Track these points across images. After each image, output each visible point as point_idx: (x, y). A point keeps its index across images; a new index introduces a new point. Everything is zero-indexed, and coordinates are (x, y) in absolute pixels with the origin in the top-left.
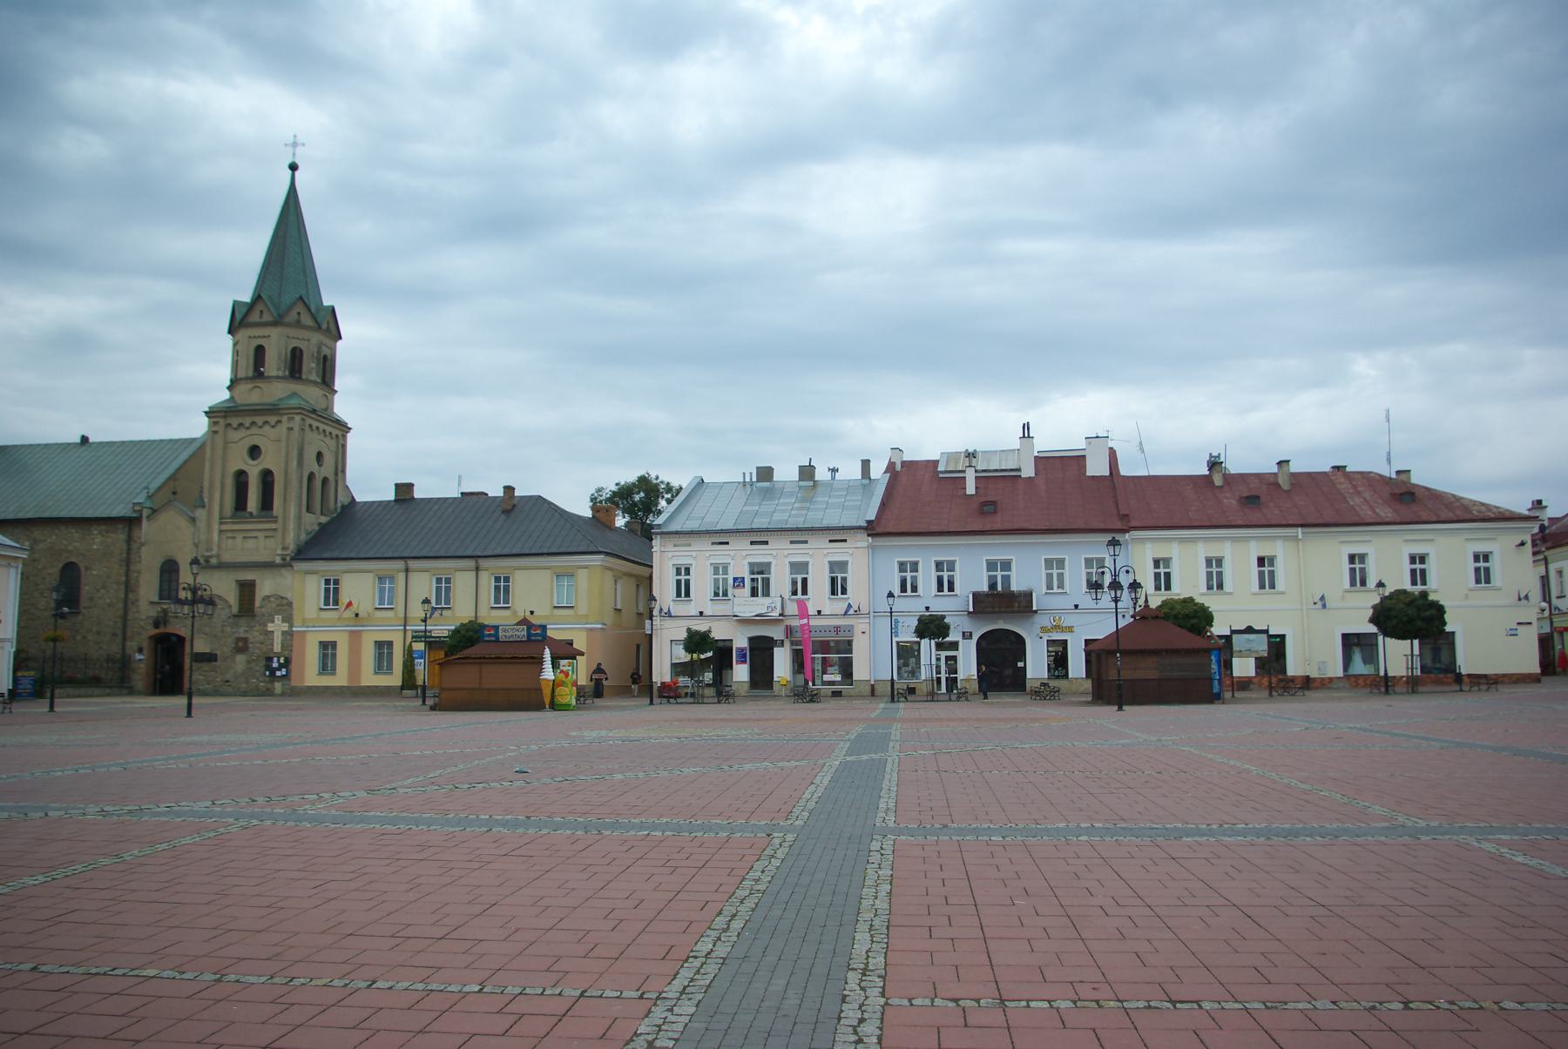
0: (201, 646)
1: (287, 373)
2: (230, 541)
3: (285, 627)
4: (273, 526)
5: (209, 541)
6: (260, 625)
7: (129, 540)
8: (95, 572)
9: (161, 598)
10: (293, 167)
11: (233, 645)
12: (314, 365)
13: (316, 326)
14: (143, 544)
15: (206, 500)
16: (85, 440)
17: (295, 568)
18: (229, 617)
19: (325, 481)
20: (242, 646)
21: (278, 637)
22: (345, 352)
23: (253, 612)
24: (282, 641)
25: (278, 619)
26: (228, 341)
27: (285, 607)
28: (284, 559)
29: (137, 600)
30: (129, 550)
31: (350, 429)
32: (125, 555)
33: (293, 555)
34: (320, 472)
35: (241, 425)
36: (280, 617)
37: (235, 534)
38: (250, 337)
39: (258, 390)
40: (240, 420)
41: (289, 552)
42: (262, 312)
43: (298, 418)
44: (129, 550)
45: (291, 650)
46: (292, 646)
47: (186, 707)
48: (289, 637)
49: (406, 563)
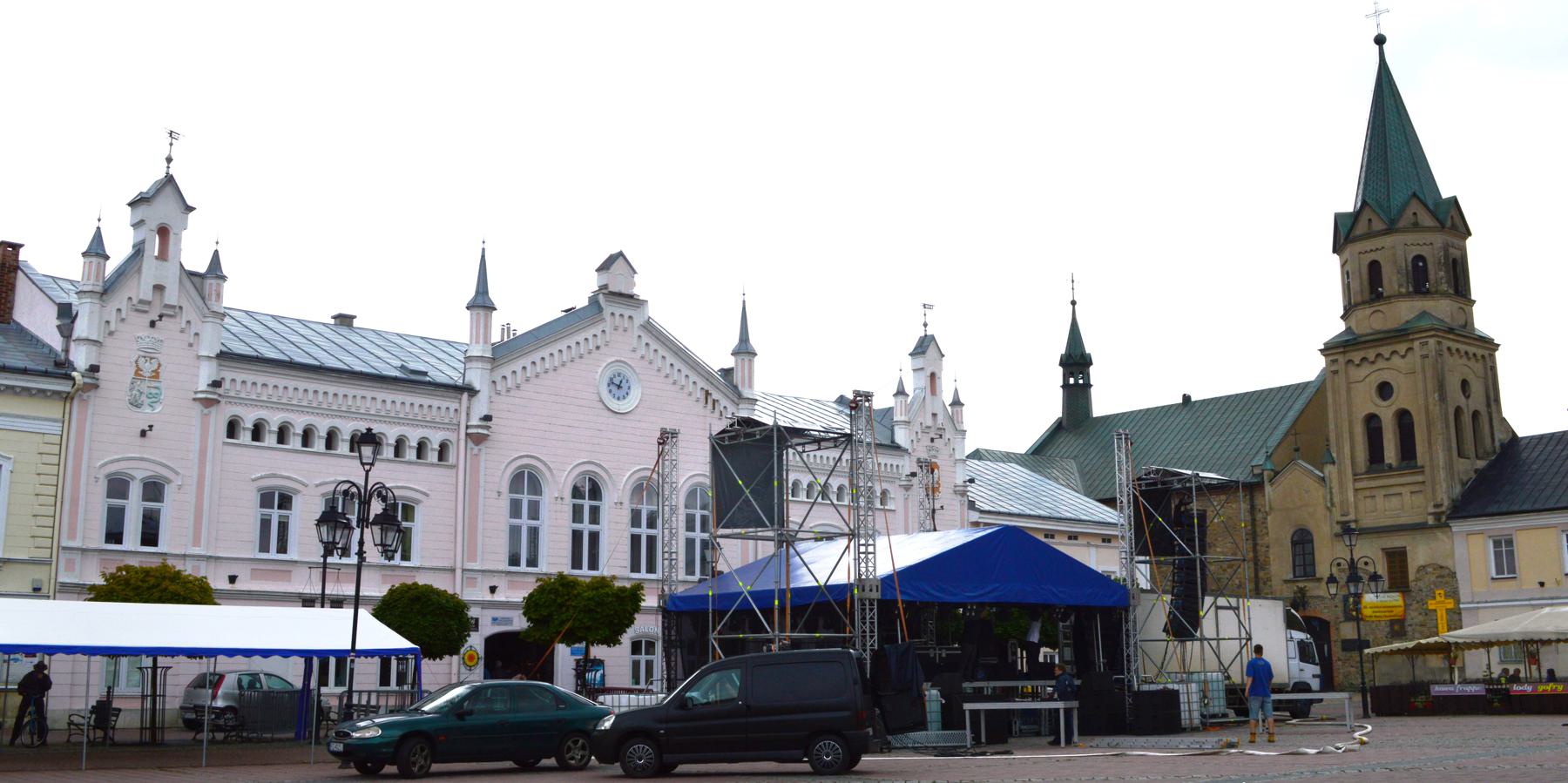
1: (1411, 289)
2: (1369, 500)
3: (1450, 604)
4: (1420, 478)
5: (1344, 502)
6: (1418, 602)
7: (1253, 509)
8: (1218, 550)
9: (1295, 576)
10: (1380, 40)
11: (1388, 629)
12: (1442, 274)
13: (1438, 225)
14: (1267, 514)
15: (1334, 455)
16: (1186, 398)
17: (1454, 529)
19: (1476, 415)
21: (1442, 616)
26: (1335, 260)
27: (1446, 578)
28: (1439, 520)
29: (1269, 579)
30: (1254, 520)
31: (1498, 345)
32: (1250, 527)
33: (1448, 512)
34: (1468, 405)
35: (1364, 359)
36: (1442, 592)
37: (1374, 492)
38: (1360, 253)
39: (1380, 314)
40: (1361, 354)
41: (1444, 509)
42: (1370, 220)
43: (1432, 341)
44: (1254, 520)
47: (1361, 704)
48: (1456, 617)
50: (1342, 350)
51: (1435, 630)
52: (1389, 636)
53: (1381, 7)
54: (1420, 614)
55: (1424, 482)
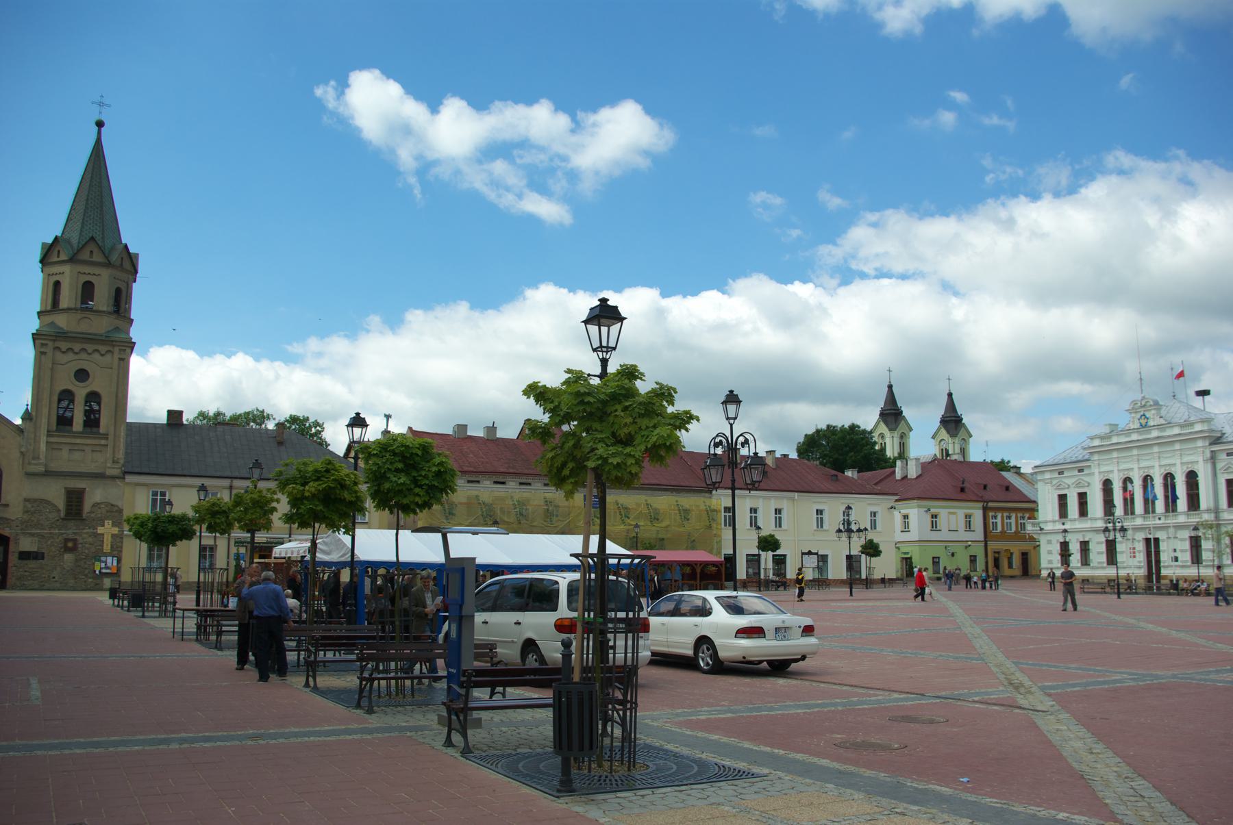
0: (27, 544)
3: (115, 530)
4: (103, 442)
10: (100, 124)
17: (127, 480)
18: (58, 520)
20: (70, 546)
21: (107, 540)
22: (138, 290)
23: (82, 517)
24: (111, 542)
25: (108, 524)
35: (70, 349)
38: (79, 272)
39: (86, 320)
40: (69, 345)
42: (91, 252)
45: (121, 551)
46: (122, 548)
48: (118, 540)
49: (232, 481)
50: (54, 338)
51: (100, 547)
52: (62, 550)
53: (106, 101)
54: (90, 536)
55: (107, 445)
